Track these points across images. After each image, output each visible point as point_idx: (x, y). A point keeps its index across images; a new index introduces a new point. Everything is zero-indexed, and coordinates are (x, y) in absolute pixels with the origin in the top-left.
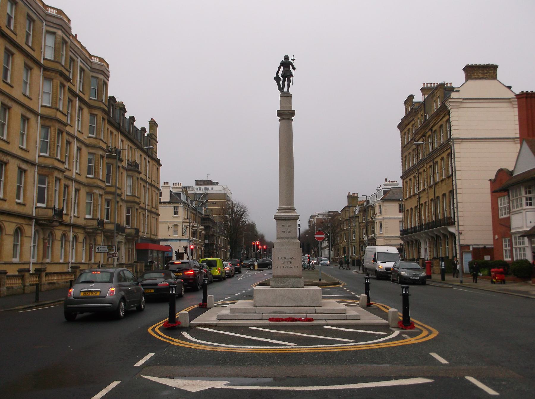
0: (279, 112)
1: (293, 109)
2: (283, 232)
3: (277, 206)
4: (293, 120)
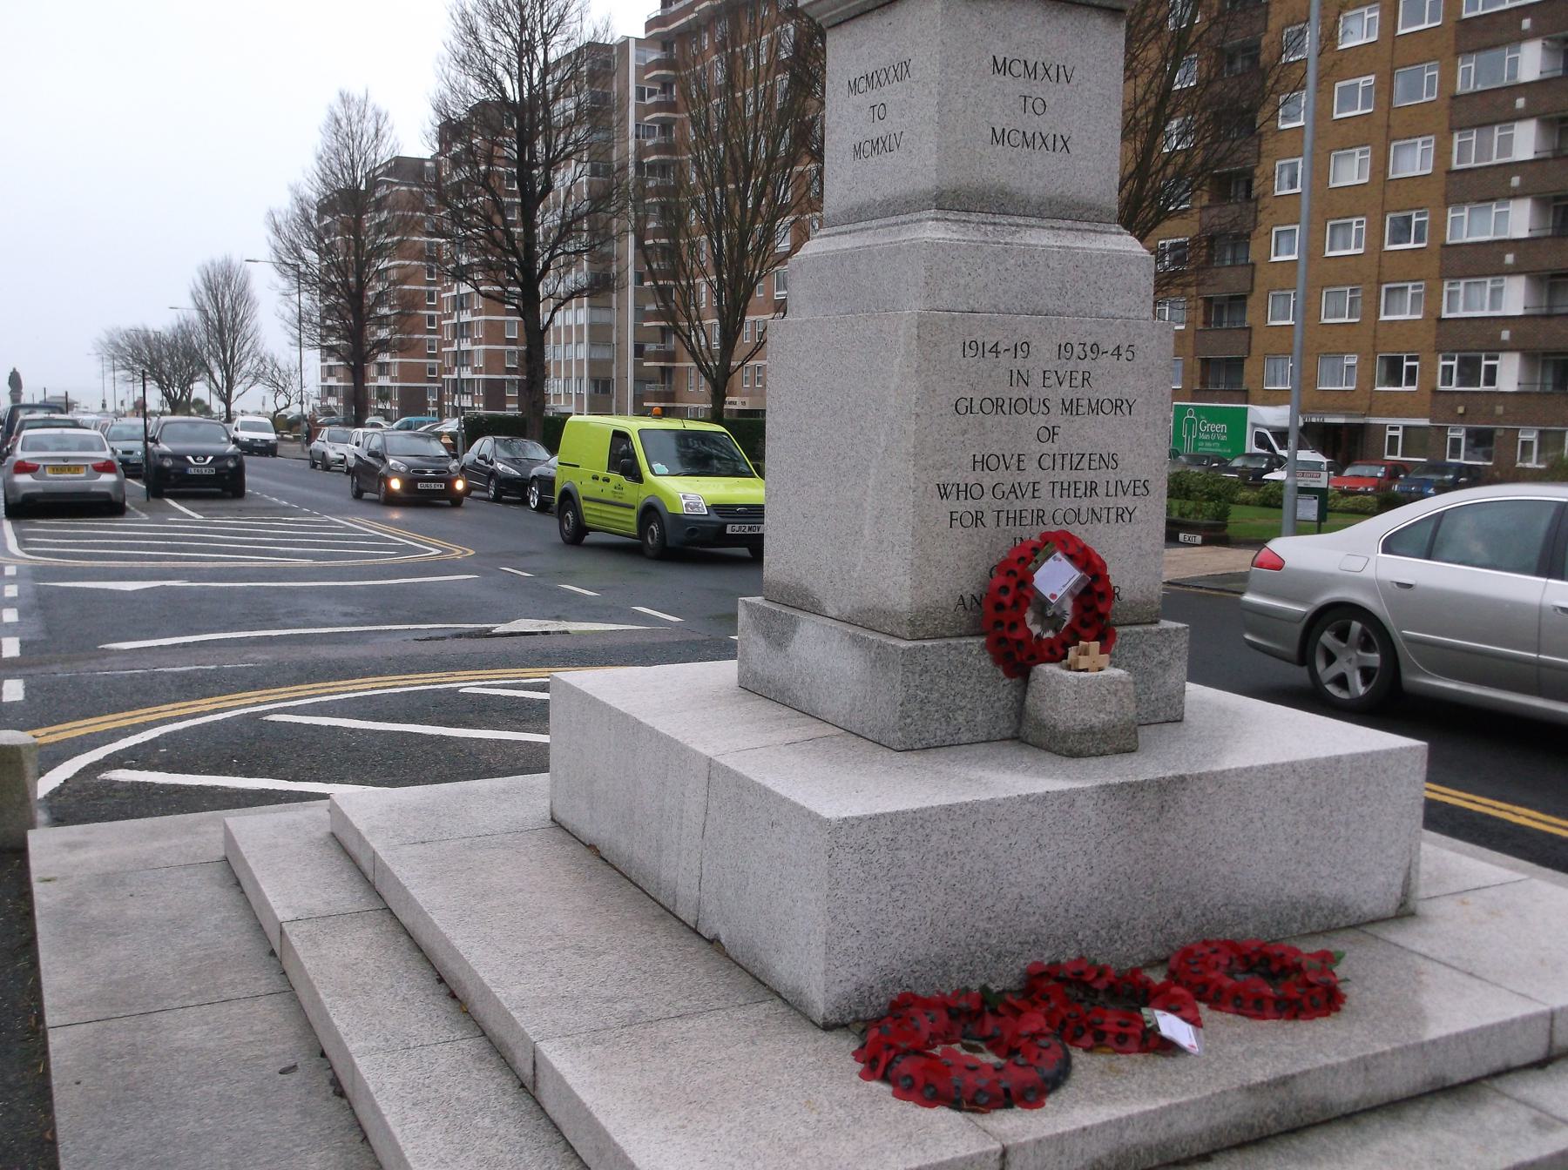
2: (999, 137)
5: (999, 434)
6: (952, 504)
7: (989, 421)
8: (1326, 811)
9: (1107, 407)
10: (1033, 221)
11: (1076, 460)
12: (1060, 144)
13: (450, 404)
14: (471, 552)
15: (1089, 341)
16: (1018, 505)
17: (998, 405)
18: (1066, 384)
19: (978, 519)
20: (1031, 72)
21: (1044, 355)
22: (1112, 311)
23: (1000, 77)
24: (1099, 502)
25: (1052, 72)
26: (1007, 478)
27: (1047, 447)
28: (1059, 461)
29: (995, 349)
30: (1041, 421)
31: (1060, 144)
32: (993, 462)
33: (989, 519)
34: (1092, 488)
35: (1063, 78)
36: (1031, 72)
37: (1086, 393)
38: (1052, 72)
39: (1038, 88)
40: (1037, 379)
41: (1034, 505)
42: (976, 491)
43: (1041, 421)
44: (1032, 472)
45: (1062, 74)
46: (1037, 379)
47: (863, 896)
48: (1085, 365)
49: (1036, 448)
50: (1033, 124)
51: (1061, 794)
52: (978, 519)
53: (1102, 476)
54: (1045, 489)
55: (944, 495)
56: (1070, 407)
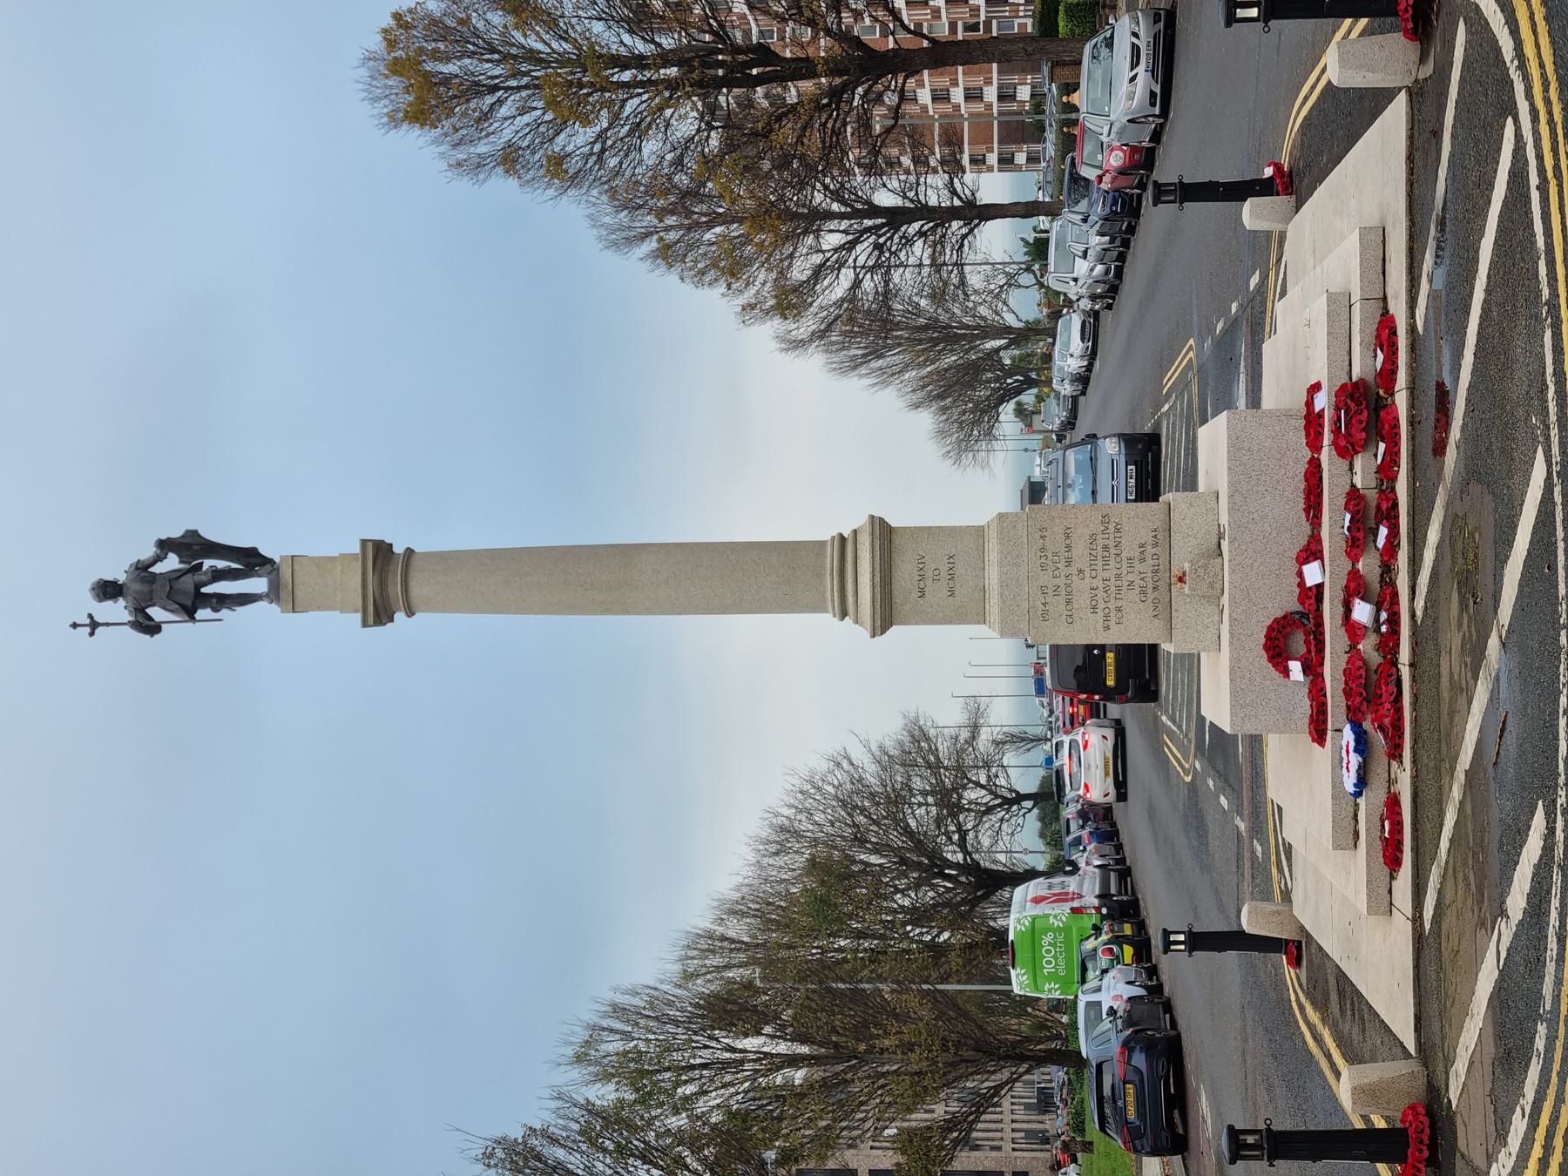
0: (371, 620)
1: (357, 549)
2: (952, 593)
3: (826, 621)
4: (410, 552)
5: (1082, 600)
6: (1112, 624)
7: (1076, 606)
8: (1253, 474)
9: (1068, 542)
10: (986, 575)
11: (1092, 558)
12: (951, 560)
13: (1022, 8)
14: (1191, 342)
15: (1039, 554)
16: (1113, 589)
17: (1069, 602)
18: (1058, 565)
19: (1119, 610)
20: (922, 578)
21: (1045, 578)
22: (1024, 536)
23: (926, 594)
24: (1111, 544)
25: (921, 566)
26: (1101, 594)
27: (1087, 574)
28: (1093, 567)
29: (1045, 604)
30: (1075, 578)
31: (951, 560)
32: (1094, 603)
33: (1119, 604)
34: (1106, 548)
35: (923, 560)
36: (922, 578)
37: (1063, 554)
38: (921, 566)
39: (929, 574)
40: (1057, 581)
41: (1113, 579)
42: (1107, 611)
43: (1075, 578)
44: (1098, 583)
45: (921, 561)
46: (1057, 581)
47: (1263, 718)
48: (1050, 555)
49: (1087, 581)
50: (944, 575)
51: (1231, 626)
52: (1119, 610)
53: (1100, 542)
54: (1106, 575)
55: (1107, 628)
56: (1069, 564)
